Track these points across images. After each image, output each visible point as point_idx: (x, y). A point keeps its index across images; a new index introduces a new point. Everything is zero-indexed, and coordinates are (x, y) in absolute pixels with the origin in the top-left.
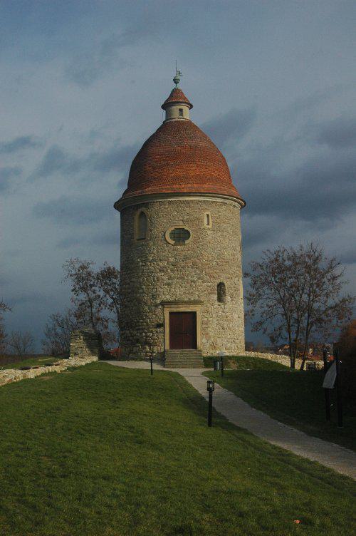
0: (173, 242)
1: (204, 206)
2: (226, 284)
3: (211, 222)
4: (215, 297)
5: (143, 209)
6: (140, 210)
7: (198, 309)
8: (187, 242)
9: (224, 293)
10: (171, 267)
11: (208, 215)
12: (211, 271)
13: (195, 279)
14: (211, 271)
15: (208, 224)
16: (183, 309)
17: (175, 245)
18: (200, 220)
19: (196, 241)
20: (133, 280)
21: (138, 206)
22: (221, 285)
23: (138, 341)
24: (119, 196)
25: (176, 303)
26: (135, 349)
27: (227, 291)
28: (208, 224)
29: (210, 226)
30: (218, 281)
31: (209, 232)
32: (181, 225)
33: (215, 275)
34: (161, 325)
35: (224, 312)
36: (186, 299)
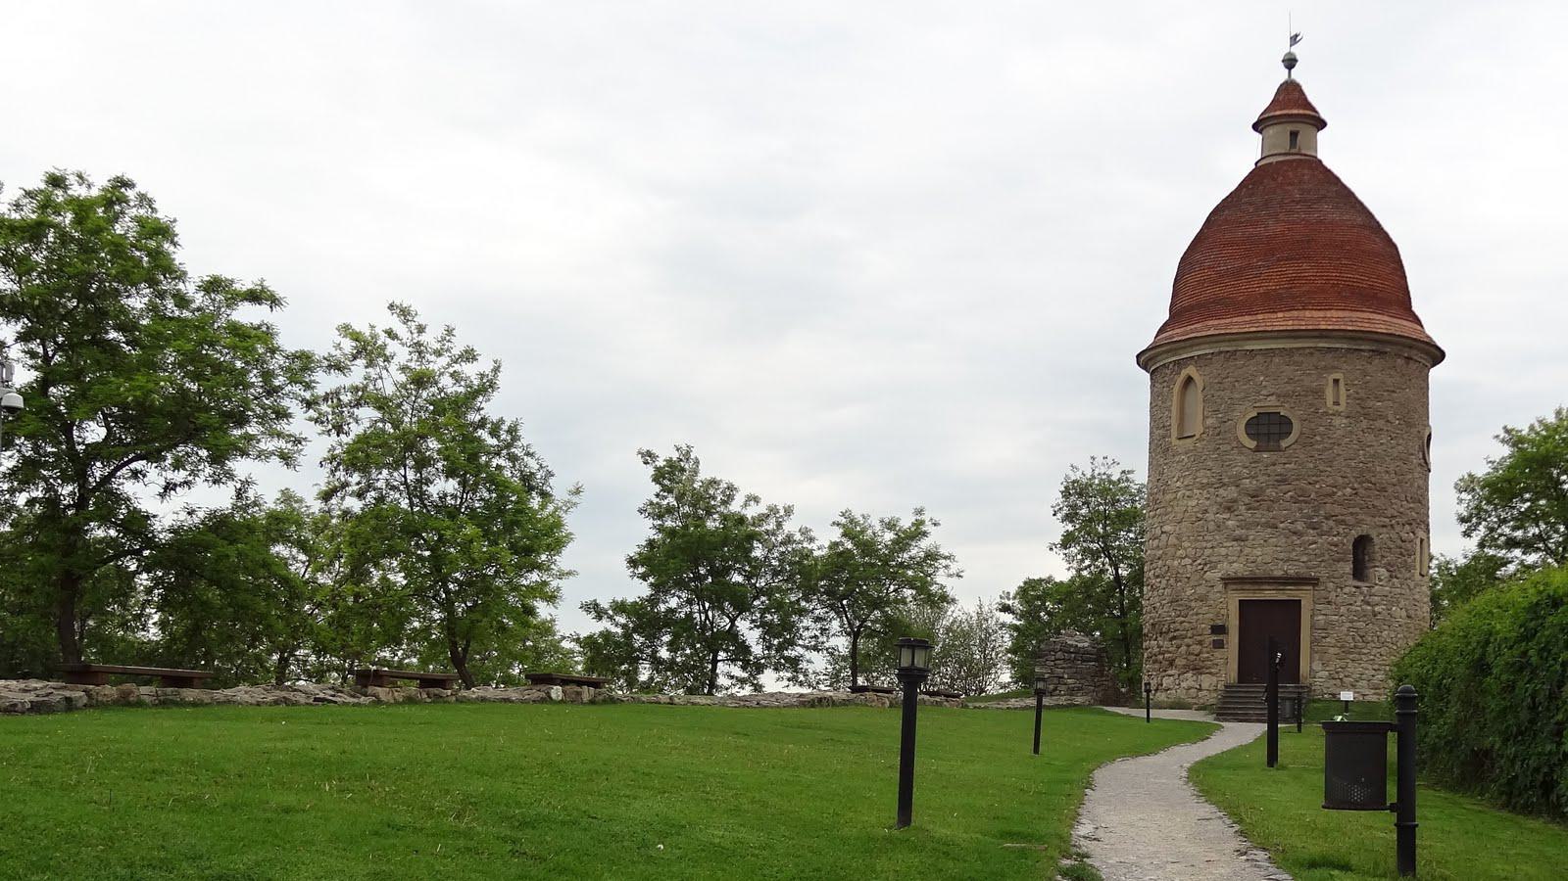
0: (1252, 444)
1: (1329, 359)
2: (1376, 540)
3: (1343, 400)
4: (1348, 568)
5: (1190, 370)
6: (1184, 373)
7: (1305, 596)
8: (1284, 444)
9: (1372, 560)
10: (1247, 500)
11: (1336, 381)
12: (1337, 509)
13: (1299, 526)
14: (1337, 509)
15: (1336, 403)
16: (1269, 594)
17: (1257, 450)
18: (1319, 393)
19: (1306, 441)
20: (1166, 528)
21: (1180, 364)
22: (1362, 543)
23: (1171, 663)
24: (1147, 340)
25: (1255, 581)
26: (1166, 682)
27: (1378, 556)
28: (1336, 403)
29: (1340, 408)
30: (1354, 534)
31: (1337, 421)
32: (1271, 404)
33: (1350, 519)
34: (1219, 630)
35: (1368, 604)
36: (1278, 573)
